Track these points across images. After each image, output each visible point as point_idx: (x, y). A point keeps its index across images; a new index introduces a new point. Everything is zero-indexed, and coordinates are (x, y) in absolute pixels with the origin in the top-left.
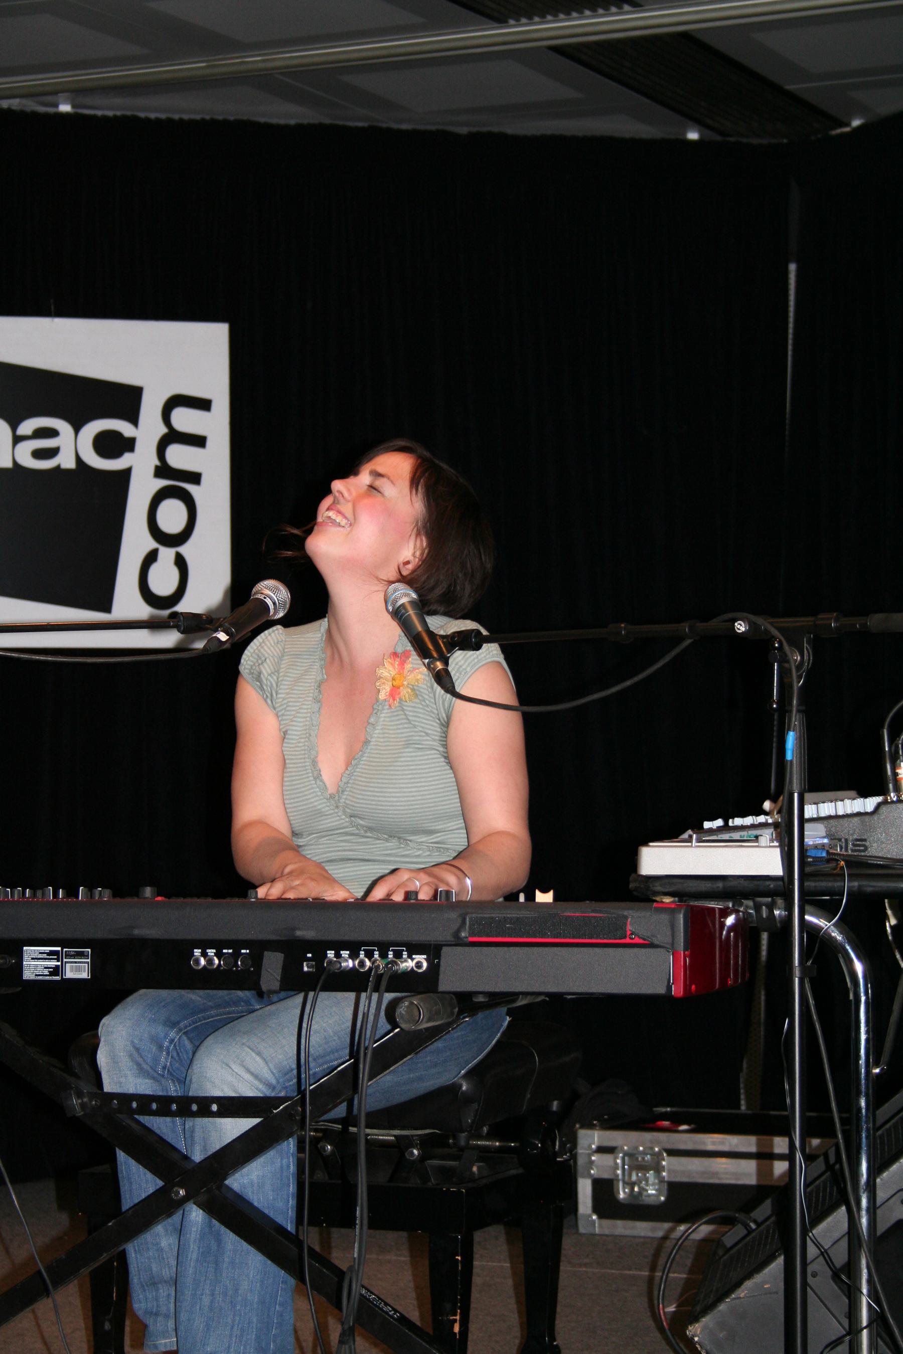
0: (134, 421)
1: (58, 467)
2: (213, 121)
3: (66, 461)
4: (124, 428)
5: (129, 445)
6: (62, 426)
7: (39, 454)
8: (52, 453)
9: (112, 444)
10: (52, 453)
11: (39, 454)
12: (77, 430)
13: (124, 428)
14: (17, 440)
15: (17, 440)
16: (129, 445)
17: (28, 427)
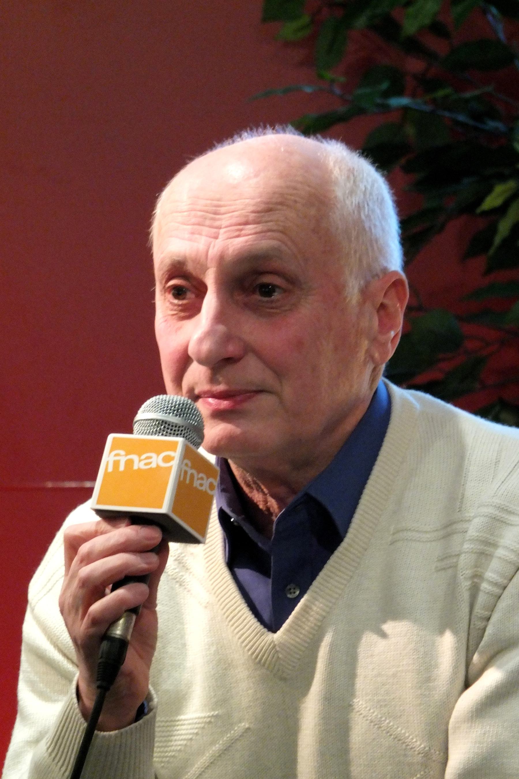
0: (175, 451)
1: (151, 468)
2: (311, 686)
3: (154, 465)
4: (172, 454)
5: (172, 459)
6: (153, 455)
7: (146, 464)
8: (150, 463)
9: (167, 459)
10: (150, 463)
11: (146, 464)
12: (158, 456)
13: (172, 454)
14: (140, 461)
15: (140, 461)
16: (172, 459)
17: (144, 456)
